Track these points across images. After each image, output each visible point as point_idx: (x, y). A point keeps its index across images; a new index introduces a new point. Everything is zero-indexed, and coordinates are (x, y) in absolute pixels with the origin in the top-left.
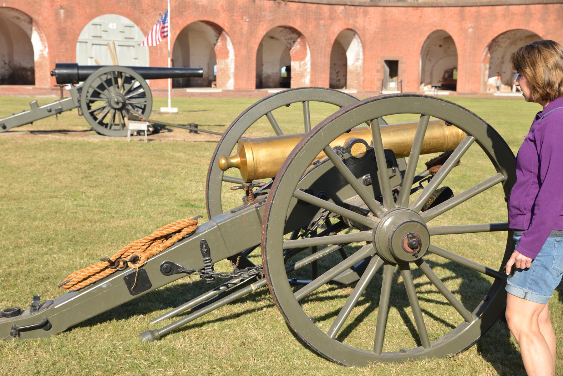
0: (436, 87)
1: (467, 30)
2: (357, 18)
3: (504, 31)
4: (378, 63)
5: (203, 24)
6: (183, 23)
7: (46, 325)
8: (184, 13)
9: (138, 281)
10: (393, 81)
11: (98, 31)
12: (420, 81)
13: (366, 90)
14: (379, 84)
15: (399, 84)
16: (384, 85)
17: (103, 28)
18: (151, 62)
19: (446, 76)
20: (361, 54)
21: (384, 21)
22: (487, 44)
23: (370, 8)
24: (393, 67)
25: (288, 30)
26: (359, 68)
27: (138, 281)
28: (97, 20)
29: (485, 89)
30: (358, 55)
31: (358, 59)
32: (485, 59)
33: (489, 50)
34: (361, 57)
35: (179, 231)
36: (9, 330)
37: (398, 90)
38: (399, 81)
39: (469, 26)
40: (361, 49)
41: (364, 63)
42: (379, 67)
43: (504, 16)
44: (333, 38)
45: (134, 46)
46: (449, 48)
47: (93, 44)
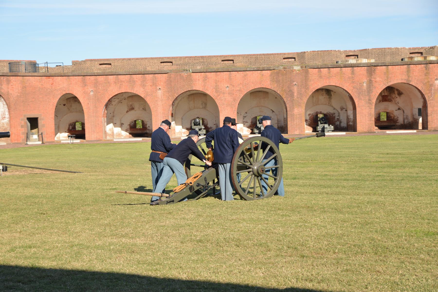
0: (72, 137)
1: (89, 93)
2: (2, 85)
3: (116, 93)
4: (22, 120)
7: (173, 201)
9: (191, 188)
10: (33, 134)
12: (54, 133)
13: (14, 142)
14: (24, 136)
15: (40, 136)
16: (27, 138)
19: (71, 128)
20: (7, 113)
21: (24, 87)
22: (105, 104)
23: (12, 77)
24: (34, 123)
26: (5, 125)
27: (191, 188)
29: (106, 137)
30: (4, 114)
31: (4, 117)
32: (104, 114)
33: (106, 108)
34: (7, 116)
35: (197, 176)
36: (166, 202)
37: (39, 141)
38: (40, 133)
39: (90, 89)
40: (7, 110)
41: (10, 121)
42: (23, 123)
43: (115, 82)
46: (71, 106)
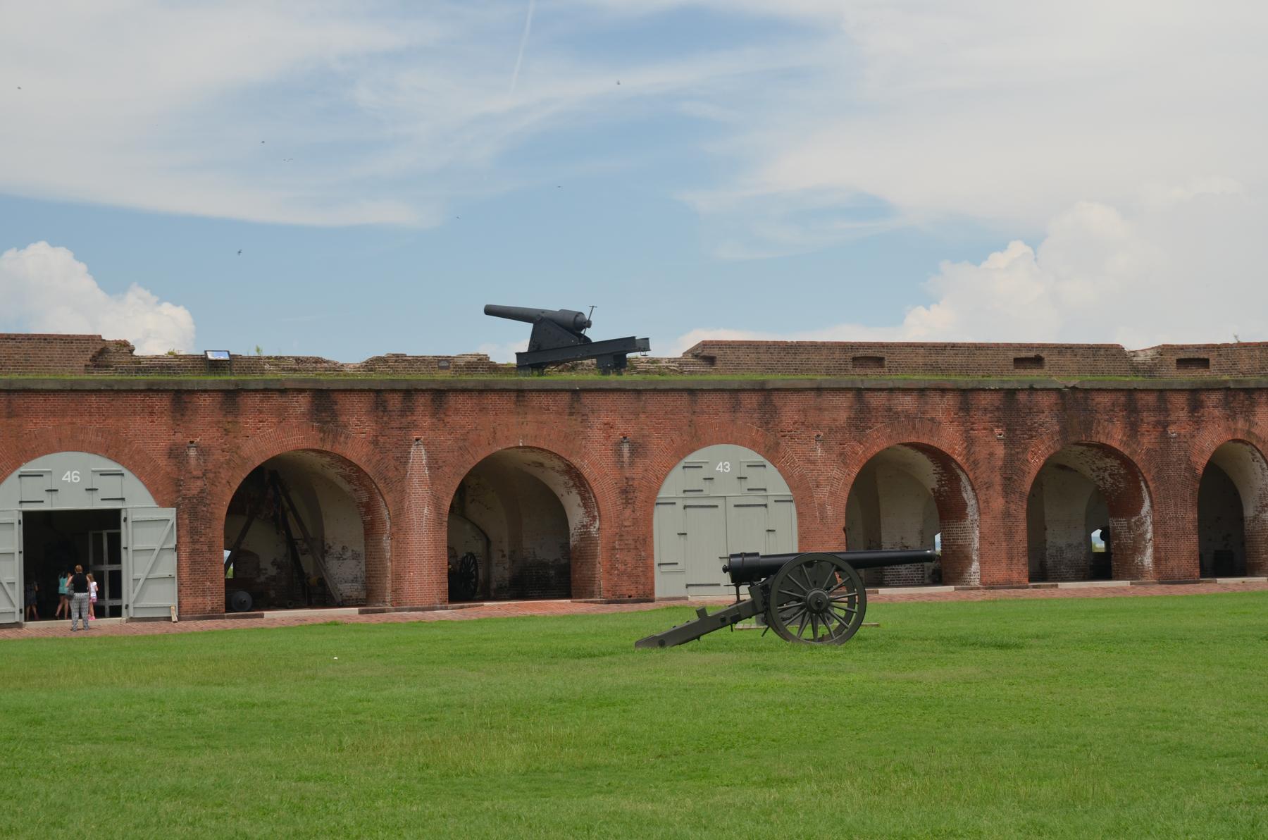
5: (907, 448)
8: (868, 431)
11: (694, 479)
17: (704, 472)
18: (802, 538)
25: (1095, 450)
28: (691, 458)
44: (1201, 462)
45: (766, 506)
47: (685, 507)
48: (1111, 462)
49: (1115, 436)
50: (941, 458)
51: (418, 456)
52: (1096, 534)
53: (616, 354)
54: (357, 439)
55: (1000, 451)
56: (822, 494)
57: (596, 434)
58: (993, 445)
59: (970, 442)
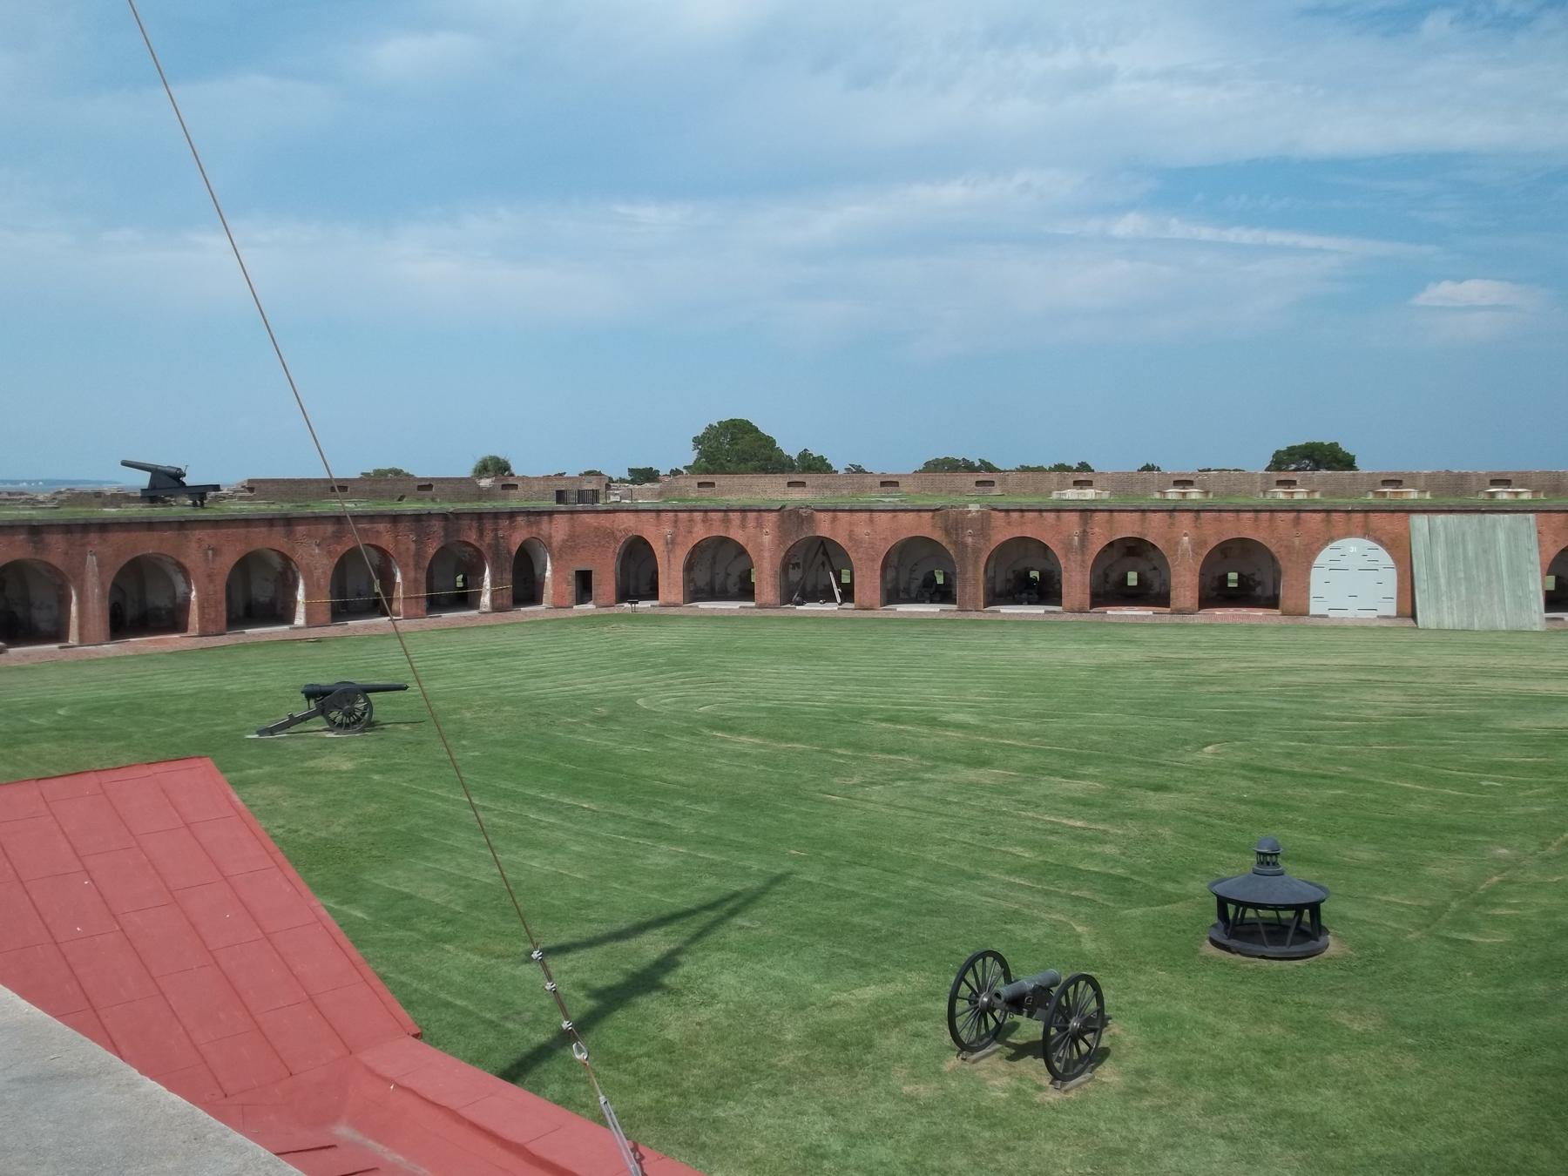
6: (342, 549)
44: (514, 549)
48: (469, 549)
49: (472, 537)
50: (383, 553)
51: (92, 561)
52: (460, 577)
53: (200, 494)
54: (56, 551)
55: (413, 546)
56: (318, 573)
57: (194, 545)
58: (409, 541)
59: (397, 542)
